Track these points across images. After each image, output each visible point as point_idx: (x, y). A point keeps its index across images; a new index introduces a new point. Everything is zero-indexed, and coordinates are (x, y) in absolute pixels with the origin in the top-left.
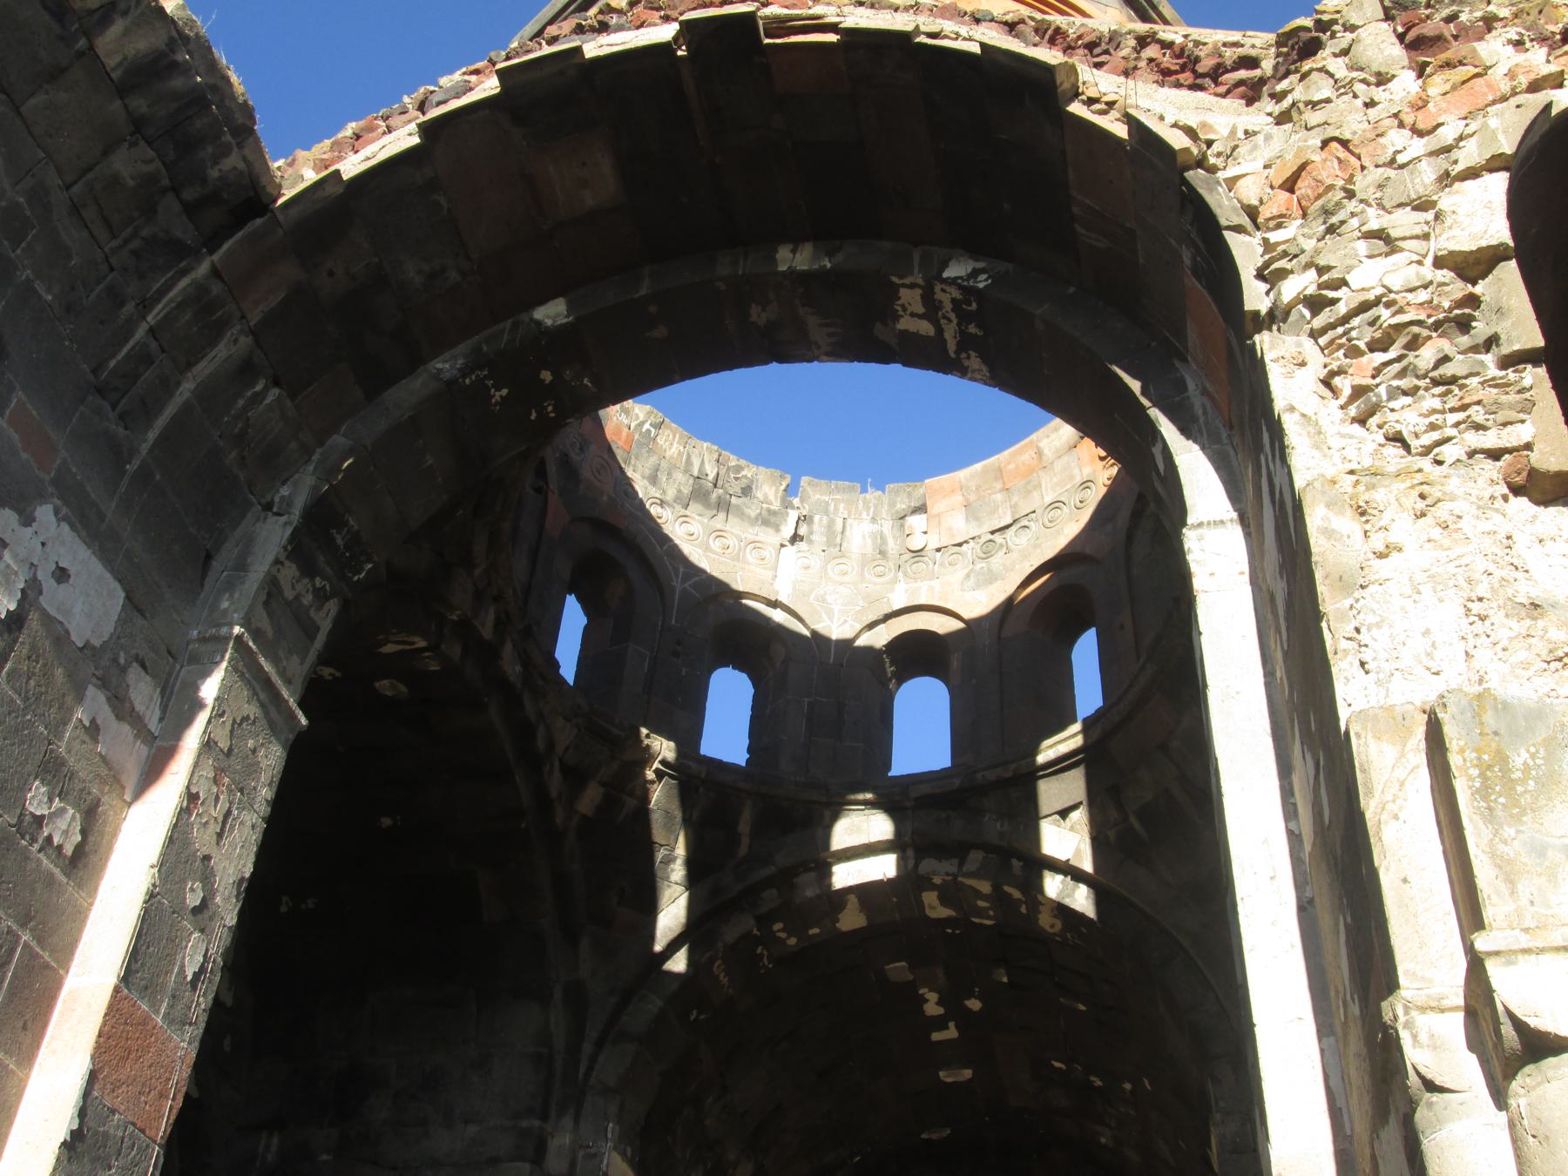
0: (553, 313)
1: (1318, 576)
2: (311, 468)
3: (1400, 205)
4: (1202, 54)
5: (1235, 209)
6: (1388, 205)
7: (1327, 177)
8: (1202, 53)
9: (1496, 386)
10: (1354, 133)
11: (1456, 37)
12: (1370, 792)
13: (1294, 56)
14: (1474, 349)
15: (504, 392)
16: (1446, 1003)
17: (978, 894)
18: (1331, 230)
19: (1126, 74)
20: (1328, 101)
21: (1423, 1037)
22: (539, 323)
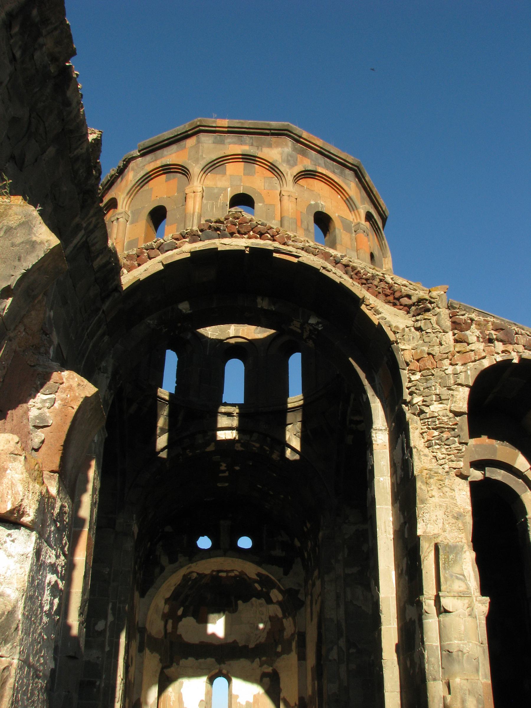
0: (184, 307)
1: (417, 498)
2: (111, 356)
3: (445, 387)
4: (396, 289)
5: (403, 361)
6: (441, 385)
7: (428, 365)
8: (396, 287)
9: (457, 450)
10: (436, 353)
11: (464, 323)
12: (422, 552)
13: (423, 310)
14: (455, 437)
15: (166, 329)
16: (431, 598)
17: (254, 446)
18: (427, 388)
19: (376, 296)
20: (430, 333)
21: (427, 604)
22: (181, 311)
